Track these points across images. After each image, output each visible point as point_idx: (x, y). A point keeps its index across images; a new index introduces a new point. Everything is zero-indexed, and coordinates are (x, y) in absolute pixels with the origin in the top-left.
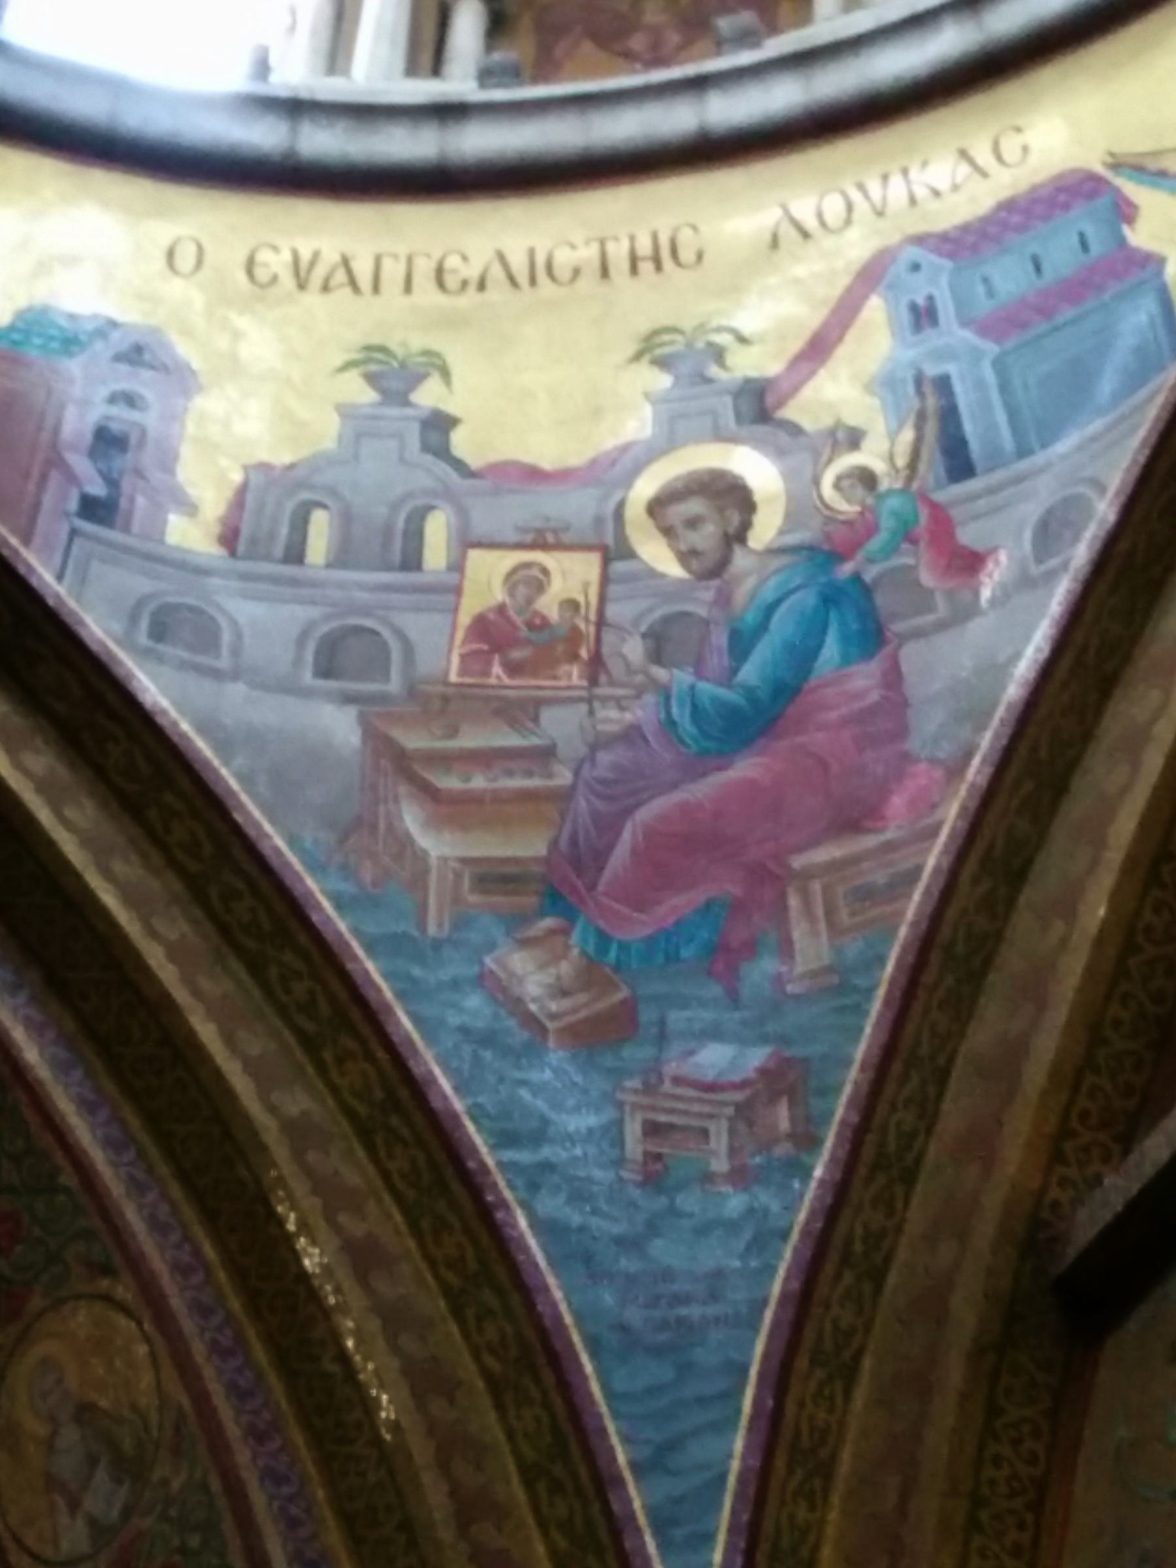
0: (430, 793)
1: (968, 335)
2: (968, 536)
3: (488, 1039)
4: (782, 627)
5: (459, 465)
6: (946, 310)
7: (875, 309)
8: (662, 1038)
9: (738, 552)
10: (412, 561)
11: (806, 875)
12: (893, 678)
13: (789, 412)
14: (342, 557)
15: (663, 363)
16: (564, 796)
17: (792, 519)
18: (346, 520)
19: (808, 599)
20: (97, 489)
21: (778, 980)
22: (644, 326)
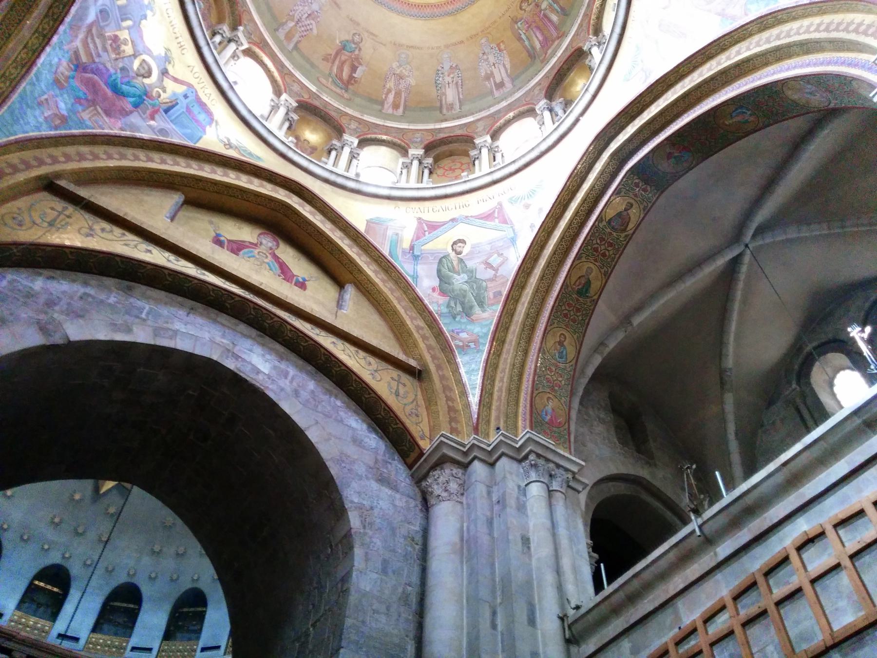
0: (87, 38)
1: (185, 106)
2: (157, 116)
3: (51, 65)
4: (132, 90)
5: (140, 23)
6: (188, 100)
8: (62, 95)
10: (123, 20)
11: (96, 109)
12: (131, 112)
15: (166, 54)
16: (94, 62)
17: (150, 86)
19: (138, 93)
21: (79, 112)
22: (170, 48)
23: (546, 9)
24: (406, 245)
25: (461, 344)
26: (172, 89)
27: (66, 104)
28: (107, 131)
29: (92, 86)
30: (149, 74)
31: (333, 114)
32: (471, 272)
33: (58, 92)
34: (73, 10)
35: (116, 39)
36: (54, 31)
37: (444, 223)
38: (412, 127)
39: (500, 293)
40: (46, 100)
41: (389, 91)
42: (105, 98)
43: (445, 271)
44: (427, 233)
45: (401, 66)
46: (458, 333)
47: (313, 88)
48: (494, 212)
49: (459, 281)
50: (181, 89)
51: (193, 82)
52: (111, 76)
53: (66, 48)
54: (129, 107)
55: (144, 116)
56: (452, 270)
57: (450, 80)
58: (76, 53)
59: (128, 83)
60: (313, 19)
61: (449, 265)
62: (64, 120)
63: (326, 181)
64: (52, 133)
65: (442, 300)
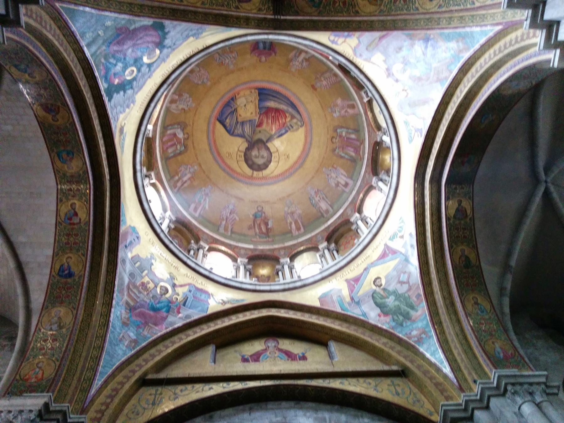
0: (129, 292)
2: (181, 311)
3: (117, 317)
4: (162, 305)
6: (192, 292)
7: (187, 287)
8: (129, 329)
9: (164, 296)
11: (149, 326)
12: (167, 316)
13: (176, 289)
14: (138, 268)
15: (170, 276)
16: (137, 302)
17: (170, 297)
18: (140, 265)
19: (166, 304)
20: (127, 245)
21: (141, 333)
23: (346, 136)
24: (348, 299)
25: (416, 339)
26: (181, 291)
27: (133, 333)
28: (159, 334)
29: (142, 315)
30: (167, 291)
31: (268, 253)
32: (395, 293)
33: (126, 328)
34: (116, 283)
35: (143, 284)
36: (112, 299)
37: (362, 274)
38: (313, 234)
39: (419, 295)
40: (123, 336)
41: (291, 224)
42: (151, 317)
43: (379, 301)
44: (355, 285)
45: (289, 208)
46: (410, 333)
47: (251, 247)
48: (385, 251)
49: (391, 301)
50: (186, 289)
51: (190, 281)
52: (149, 304)
53: (121, 303)
54: (165, 314)
55: (175, 314)
56: (383, 297)
57: (319, 199)
58: (127, 303)
59: (159, 303)
60: (233, 213)
61: (379, 296)
62: (136, 342)
63: (284, 290)
64: (133, 352)
65: (388, 319)
